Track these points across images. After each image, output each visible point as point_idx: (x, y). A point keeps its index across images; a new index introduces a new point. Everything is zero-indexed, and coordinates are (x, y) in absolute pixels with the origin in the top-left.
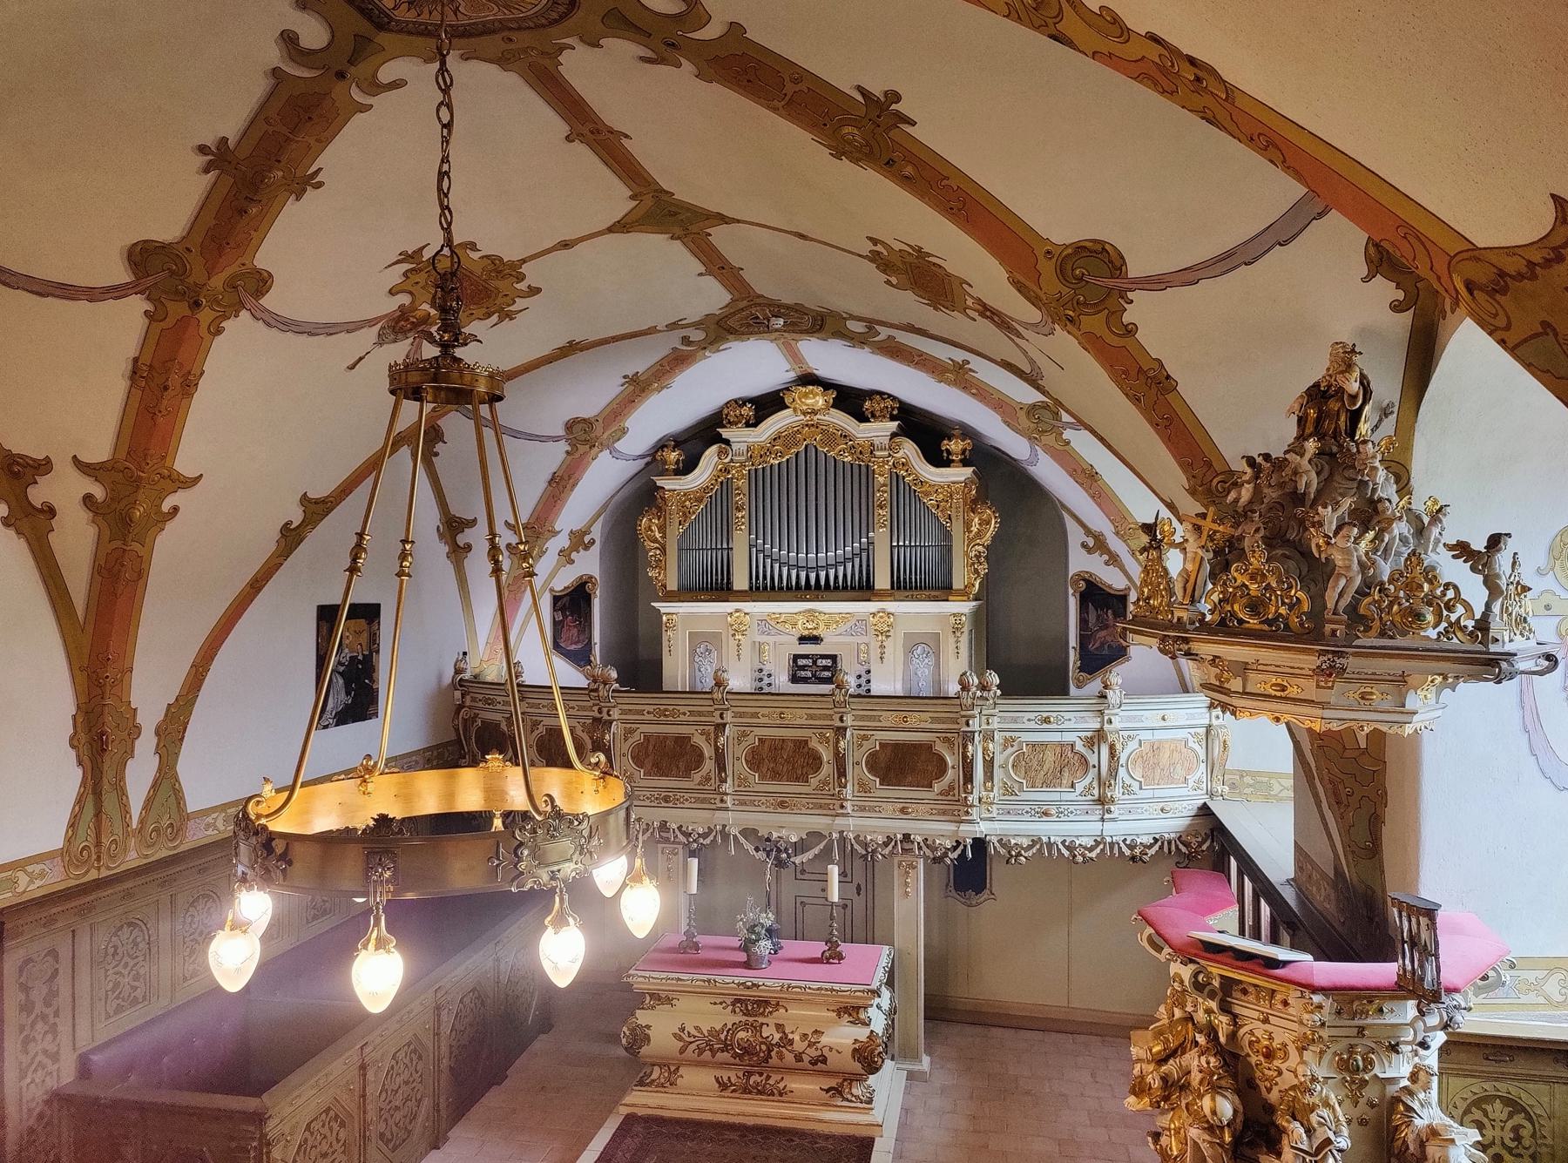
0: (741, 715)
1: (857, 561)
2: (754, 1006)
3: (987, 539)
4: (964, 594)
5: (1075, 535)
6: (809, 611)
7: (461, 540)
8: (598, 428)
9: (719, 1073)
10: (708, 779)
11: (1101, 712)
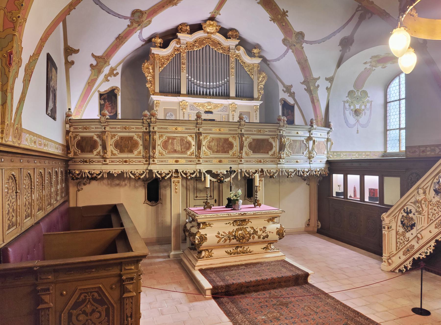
0: (205, 130)
1: (223, 86)
2: (241, 222)
3: (263, 83)
4: (257, 99)
5: (281, 87)
6: (209, 102)
7: (70, 59)
8: (145, 16)
9: (226, 250)
10: (192, 154)
11: (310, 132)
